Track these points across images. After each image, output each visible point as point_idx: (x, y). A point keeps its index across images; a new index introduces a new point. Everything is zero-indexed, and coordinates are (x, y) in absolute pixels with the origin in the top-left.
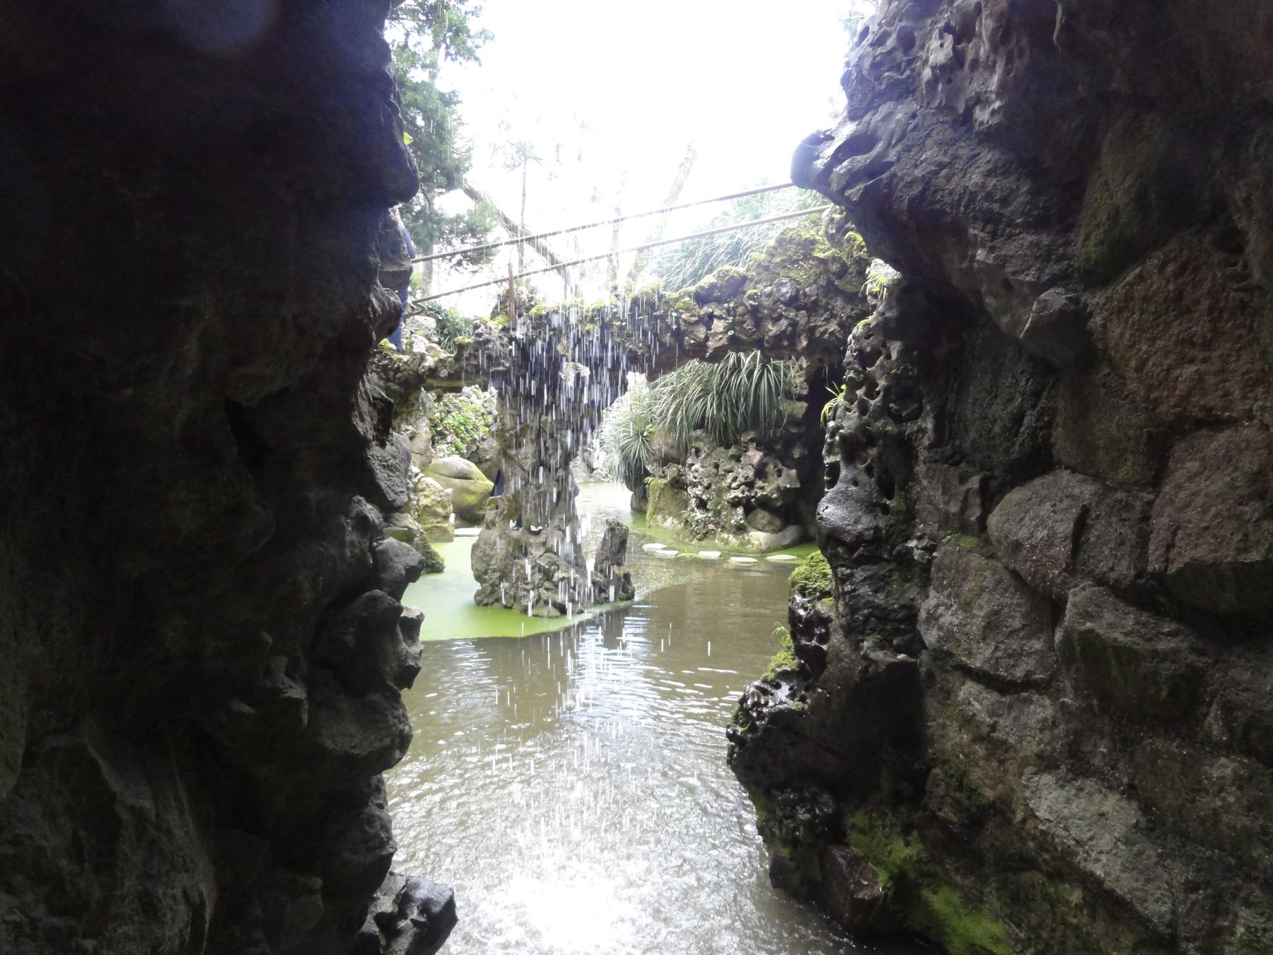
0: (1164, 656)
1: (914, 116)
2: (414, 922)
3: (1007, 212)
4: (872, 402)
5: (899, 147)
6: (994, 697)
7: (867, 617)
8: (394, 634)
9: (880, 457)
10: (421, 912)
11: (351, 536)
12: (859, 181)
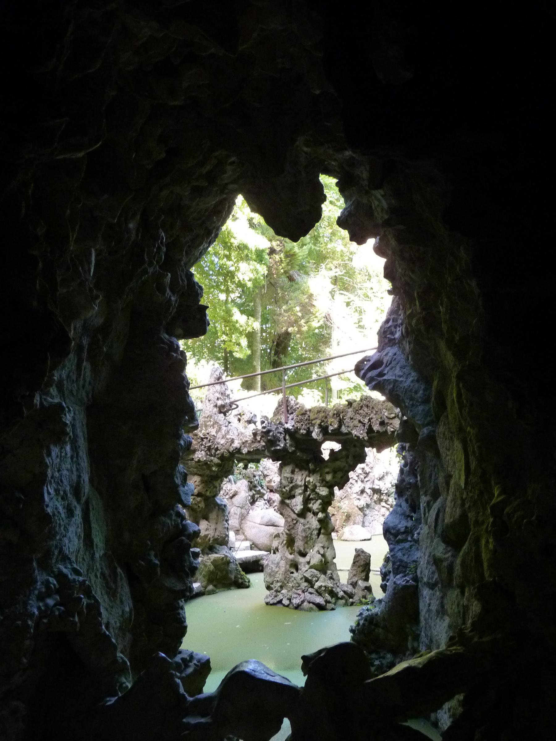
0: (447, 559)
1: (395, 354)
2: (195, 664)
4: (405, 469)
6: (431, 592)
7: (399, 566)
9: (411, 495)
10: (198, 662)
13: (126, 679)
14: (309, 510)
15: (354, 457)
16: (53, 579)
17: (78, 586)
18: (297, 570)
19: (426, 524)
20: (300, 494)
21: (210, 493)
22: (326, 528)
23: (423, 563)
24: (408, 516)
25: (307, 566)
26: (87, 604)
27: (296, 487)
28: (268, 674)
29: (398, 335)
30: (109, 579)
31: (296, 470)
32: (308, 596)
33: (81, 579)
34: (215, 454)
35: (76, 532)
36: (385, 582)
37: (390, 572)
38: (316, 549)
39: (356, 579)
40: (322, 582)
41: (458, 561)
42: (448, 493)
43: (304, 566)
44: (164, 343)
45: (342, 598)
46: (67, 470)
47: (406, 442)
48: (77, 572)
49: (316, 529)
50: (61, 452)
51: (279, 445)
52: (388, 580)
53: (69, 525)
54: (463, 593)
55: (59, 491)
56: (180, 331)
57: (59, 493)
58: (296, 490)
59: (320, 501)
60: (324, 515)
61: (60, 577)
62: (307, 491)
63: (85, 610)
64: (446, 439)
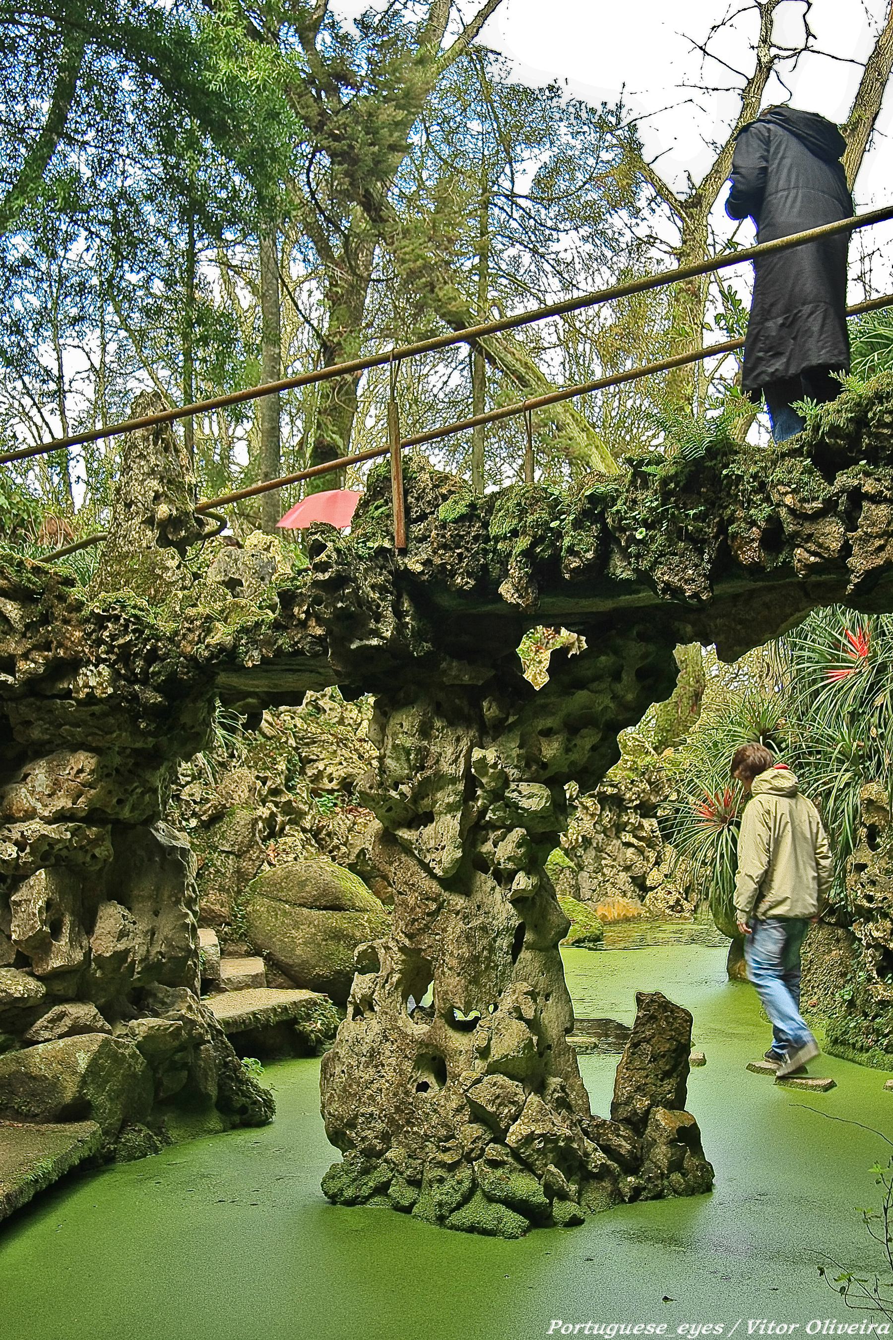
14: (482, 864)
15: (641, 674)
20: (451, 808)
22: (539, 925)
25: (480, 1065)
27: (439, 781)
31: (438, 724)
34: (145, 671)
38: (507, 1002)
40: (532, 1119)
45: (604, 1172)
49: (508, 929)
51: (376, 633)
58: (439, 795)
59: (518, 832)
60: (534, 880)
62: (475, 799)
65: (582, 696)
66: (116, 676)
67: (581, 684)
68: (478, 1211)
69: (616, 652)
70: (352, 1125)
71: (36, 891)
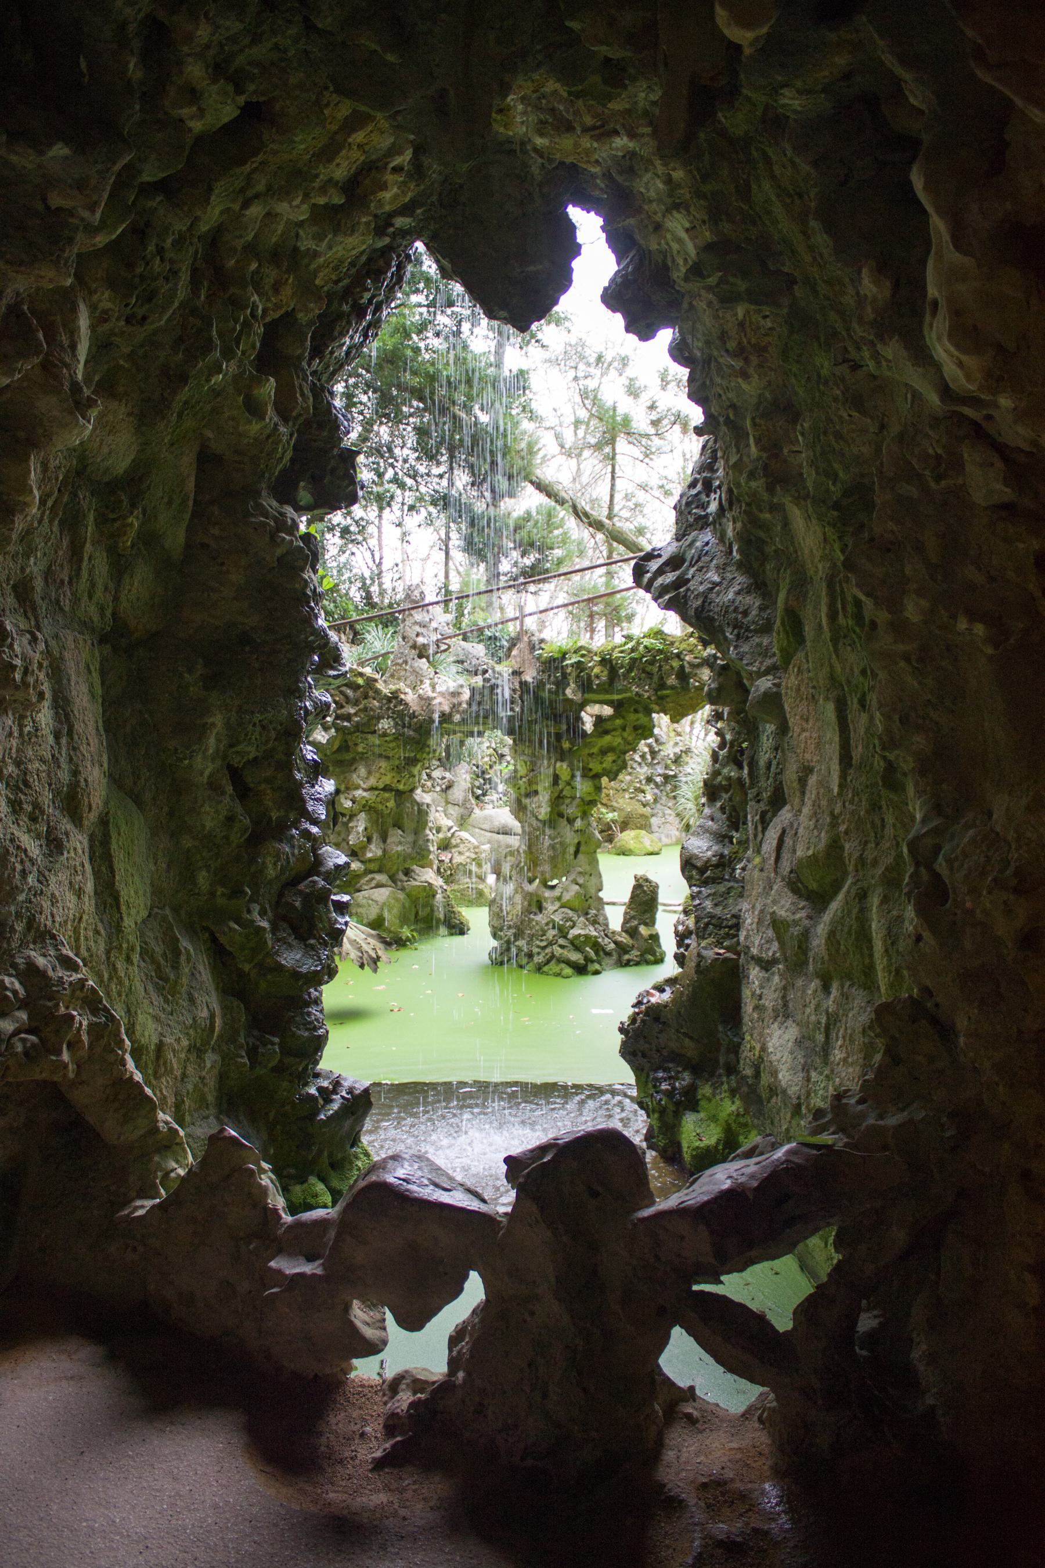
0: (796, 923)
1: (707, 544)
3: (745, 621)
5: (695, 568)
7: (707, 924)
8: (326, 906)
9: (730, 799)
10: (348, 1093)
11: (299, 841)
12: (667, 592)
13: (177, 1162)
16: (13, 979)
17: (67, 992)
18: (540, 908)
19: (759, 852)
21: (405, 784)
23: (749, 920)
24: (725, 836)
25: (557, 904)
26: (90, 1025)
28: (436, 1185)
29: (713, 507)
30: (162, 962)
32: (558, 951)
33: (75, 977)
34: (410, 724)
35: (71, 883)
36: (682, 950)
37: (690, 933)
39: (636, 922)
41: (822, 929)
42: (803, 801)
43: (553, 903)
44: (266, 515)
46: (42, 760)
47: (724, 704)
48: (68, 964)
50: (21, 727)
52: (688, 946)
53: (50, 871)
54: (826, 988)
55: (21, 803)
56: (304, 496)
57: (21, 808)
61: (31, 974)
63: (85, 1038)
64: (802, 699)
65: (608, 738)
66: (396, 724)
67: (606, 732)
68: (553, 967)
69: (623, 718)
70: (501, 930)
71: (360, 824)
